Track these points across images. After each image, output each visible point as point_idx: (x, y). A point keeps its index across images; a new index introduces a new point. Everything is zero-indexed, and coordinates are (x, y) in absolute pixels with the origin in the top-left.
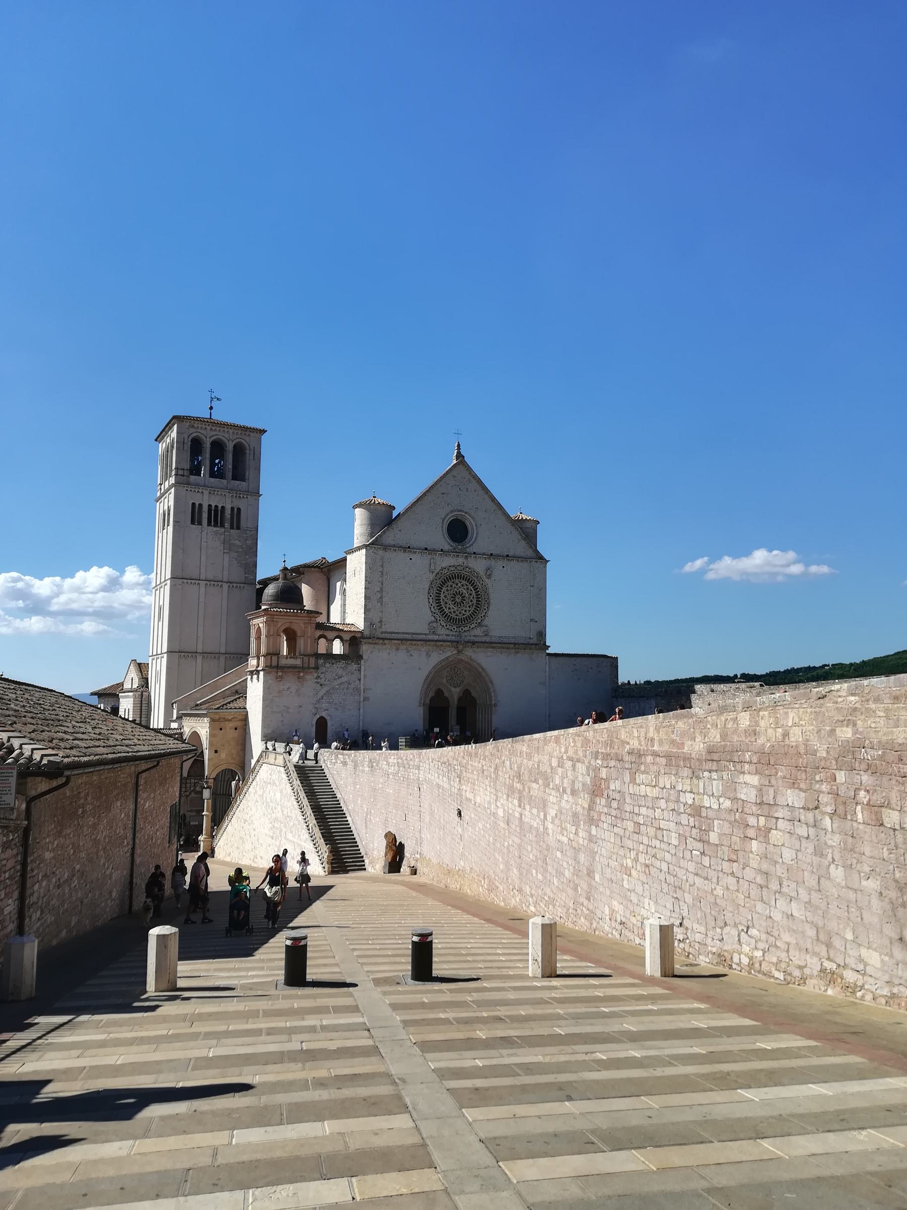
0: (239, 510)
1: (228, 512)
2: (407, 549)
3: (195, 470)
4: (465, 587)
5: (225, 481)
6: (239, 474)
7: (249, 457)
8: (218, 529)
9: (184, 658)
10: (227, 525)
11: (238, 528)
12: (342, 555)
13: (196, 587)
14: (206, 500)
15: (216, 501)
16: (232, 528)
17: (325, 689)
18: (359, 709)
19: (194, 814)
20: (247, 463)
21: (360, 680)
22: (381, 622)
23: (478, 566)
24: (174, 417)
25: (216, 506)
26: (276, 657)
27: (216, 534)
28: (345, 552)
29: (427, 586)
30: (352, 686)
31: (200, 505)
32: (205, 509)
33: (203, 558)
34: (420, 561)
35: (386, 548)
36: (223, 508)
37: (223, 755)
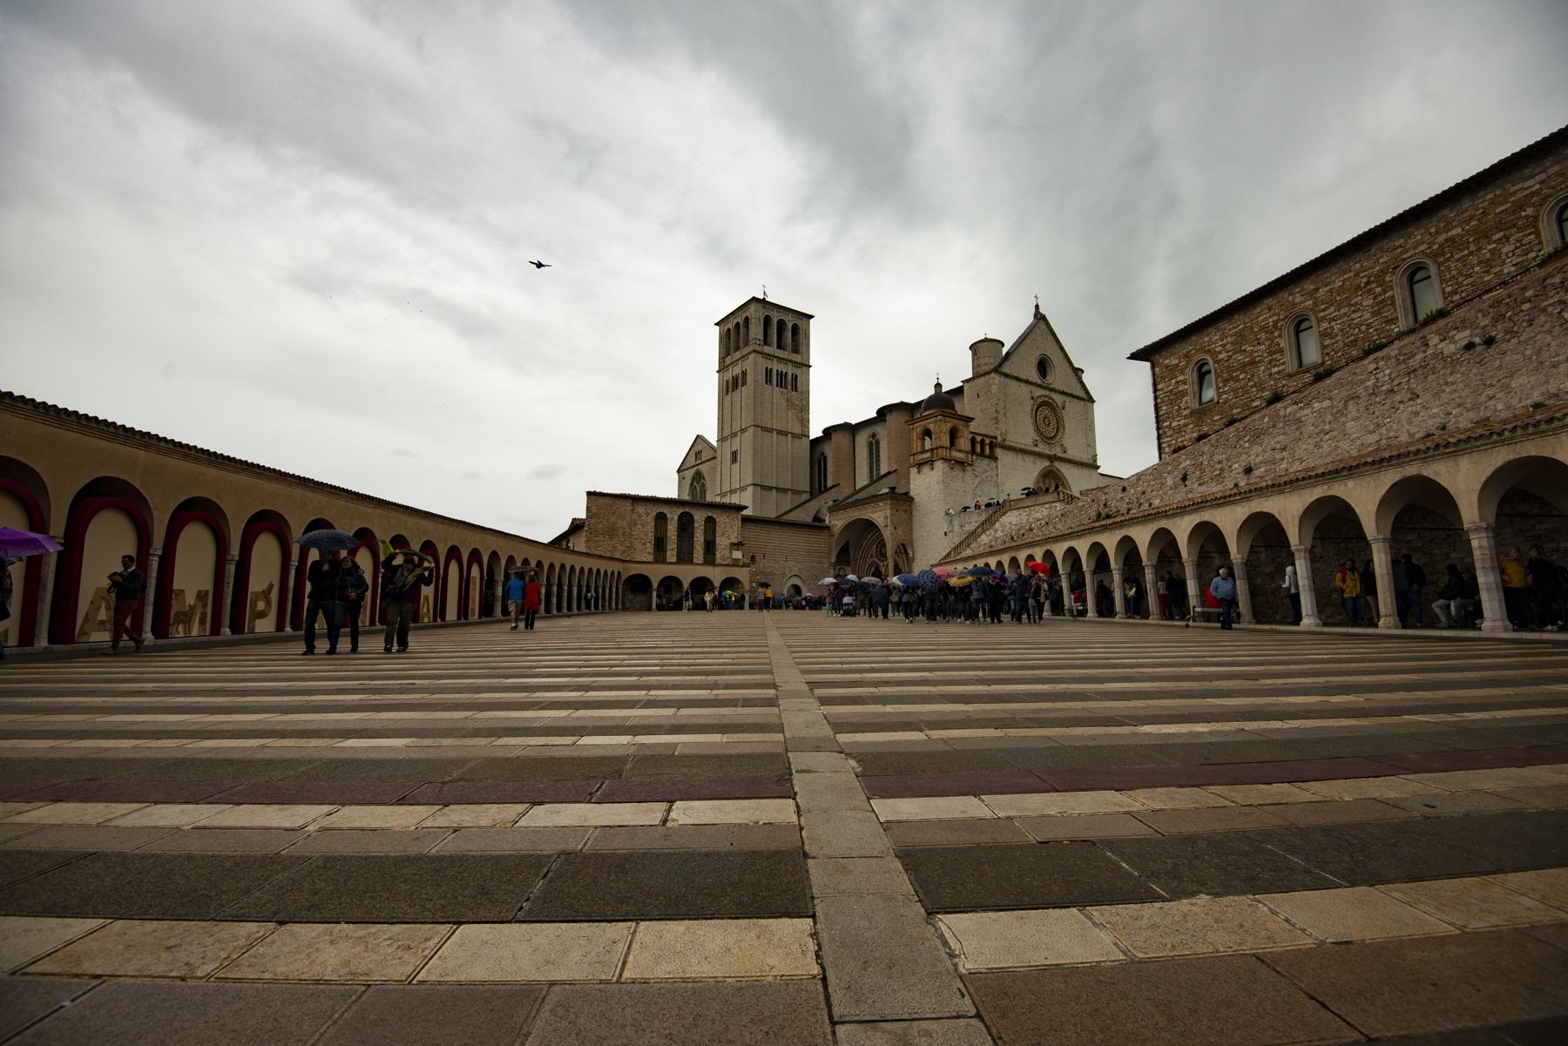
0: (796, 376)
1: (790, 377)
2: (1018, 379)
3: (766, 342)
11: (796, 391)
13: (770, 434)
14: (776, 366)
15: (782, 368)
17: (979, 479)
23: (1058, 399)
24: (754, 298)
25: (782, 372)
28: (962, 382)
29: (1029, 409)
30: (994, 480)
33: (775, 411)
35: (1006, 375)
36: (786, 373)
37: (900, 532)
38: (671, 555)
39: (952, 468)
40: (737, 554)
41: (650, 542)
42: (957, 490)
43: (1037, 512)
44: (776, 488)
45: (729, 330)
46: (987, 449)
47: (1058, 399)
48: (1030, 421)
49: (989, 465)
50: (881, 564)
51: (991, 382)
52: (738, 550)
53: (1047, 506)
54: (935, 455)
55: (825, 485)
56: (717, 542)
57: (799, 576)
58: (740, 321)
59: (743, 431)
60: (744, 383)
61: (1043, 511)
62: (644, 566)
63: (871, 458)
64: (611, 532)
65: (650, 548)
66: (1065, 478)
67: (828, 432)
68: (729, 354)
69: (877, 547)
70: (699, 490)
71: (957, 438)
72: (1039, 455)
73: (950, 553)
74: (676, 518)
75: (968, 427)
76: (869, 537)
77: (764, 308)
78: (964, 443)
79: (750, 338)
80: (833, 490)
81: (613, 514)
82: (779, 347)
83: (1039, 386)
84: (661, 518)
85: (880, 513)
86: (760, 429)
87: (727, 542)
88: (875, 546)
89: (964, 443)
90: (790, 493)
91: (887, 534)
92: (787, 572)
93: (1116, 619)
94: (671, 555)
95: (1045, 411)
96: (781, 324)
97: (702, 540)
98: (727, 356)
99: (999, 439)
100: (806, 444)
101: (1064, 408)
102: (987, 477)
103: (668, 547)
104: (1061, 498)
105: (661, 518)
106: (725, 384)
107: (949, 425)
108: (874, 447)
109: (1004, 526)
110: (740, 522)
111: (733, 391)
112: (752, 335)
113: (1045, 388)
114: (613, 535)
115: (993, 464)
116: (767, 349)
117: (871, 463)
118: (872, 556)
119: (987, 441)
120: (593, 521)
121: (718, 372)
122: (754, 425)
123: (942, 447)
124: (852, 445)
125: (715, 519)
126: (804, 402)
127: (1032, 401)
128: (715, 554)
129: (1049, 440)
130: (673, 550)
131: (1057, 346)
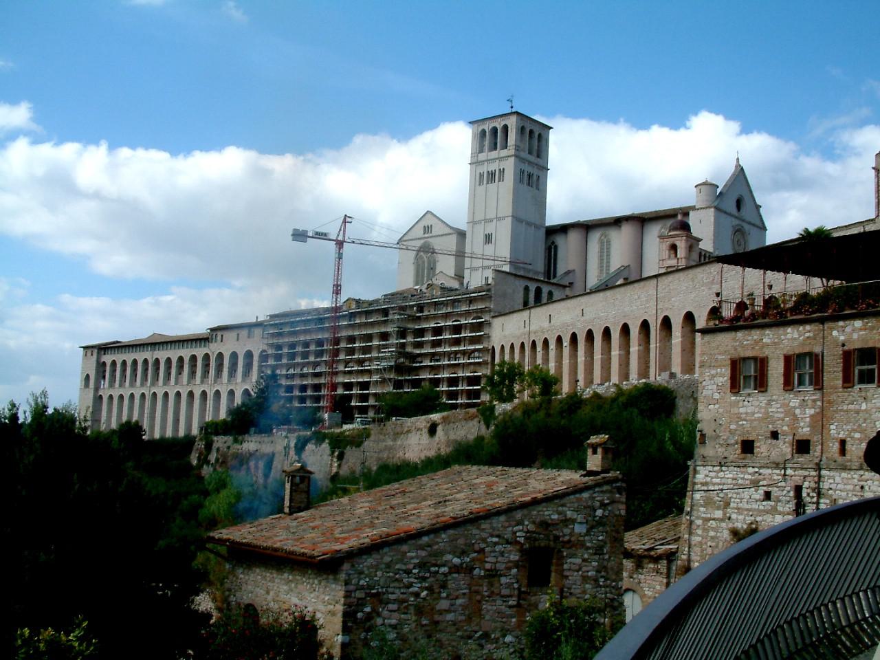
1: (535, 178)
2: (725, 213)
6: (538, 156)
10: (534, 186)
14: (528, 169)
23: (746, 227)
32: (526, 174)
34: (729, 219)
45: (483, 132)
58: (498, 127)
59: (499, 219)
67: (564, 229)
70: (426, 259)
74: (534, 290)
75: (698, 245)
77: (522, 119)
78: (695, 256)
80: (571, 274)
83: (736, 217)
95: (738, 236)
96: (531, 132)
100: (542, 233)
105: (527, 289)
107: (689, 243)
119: (707, 255)
121: (470, 164)
127: (731, 229)
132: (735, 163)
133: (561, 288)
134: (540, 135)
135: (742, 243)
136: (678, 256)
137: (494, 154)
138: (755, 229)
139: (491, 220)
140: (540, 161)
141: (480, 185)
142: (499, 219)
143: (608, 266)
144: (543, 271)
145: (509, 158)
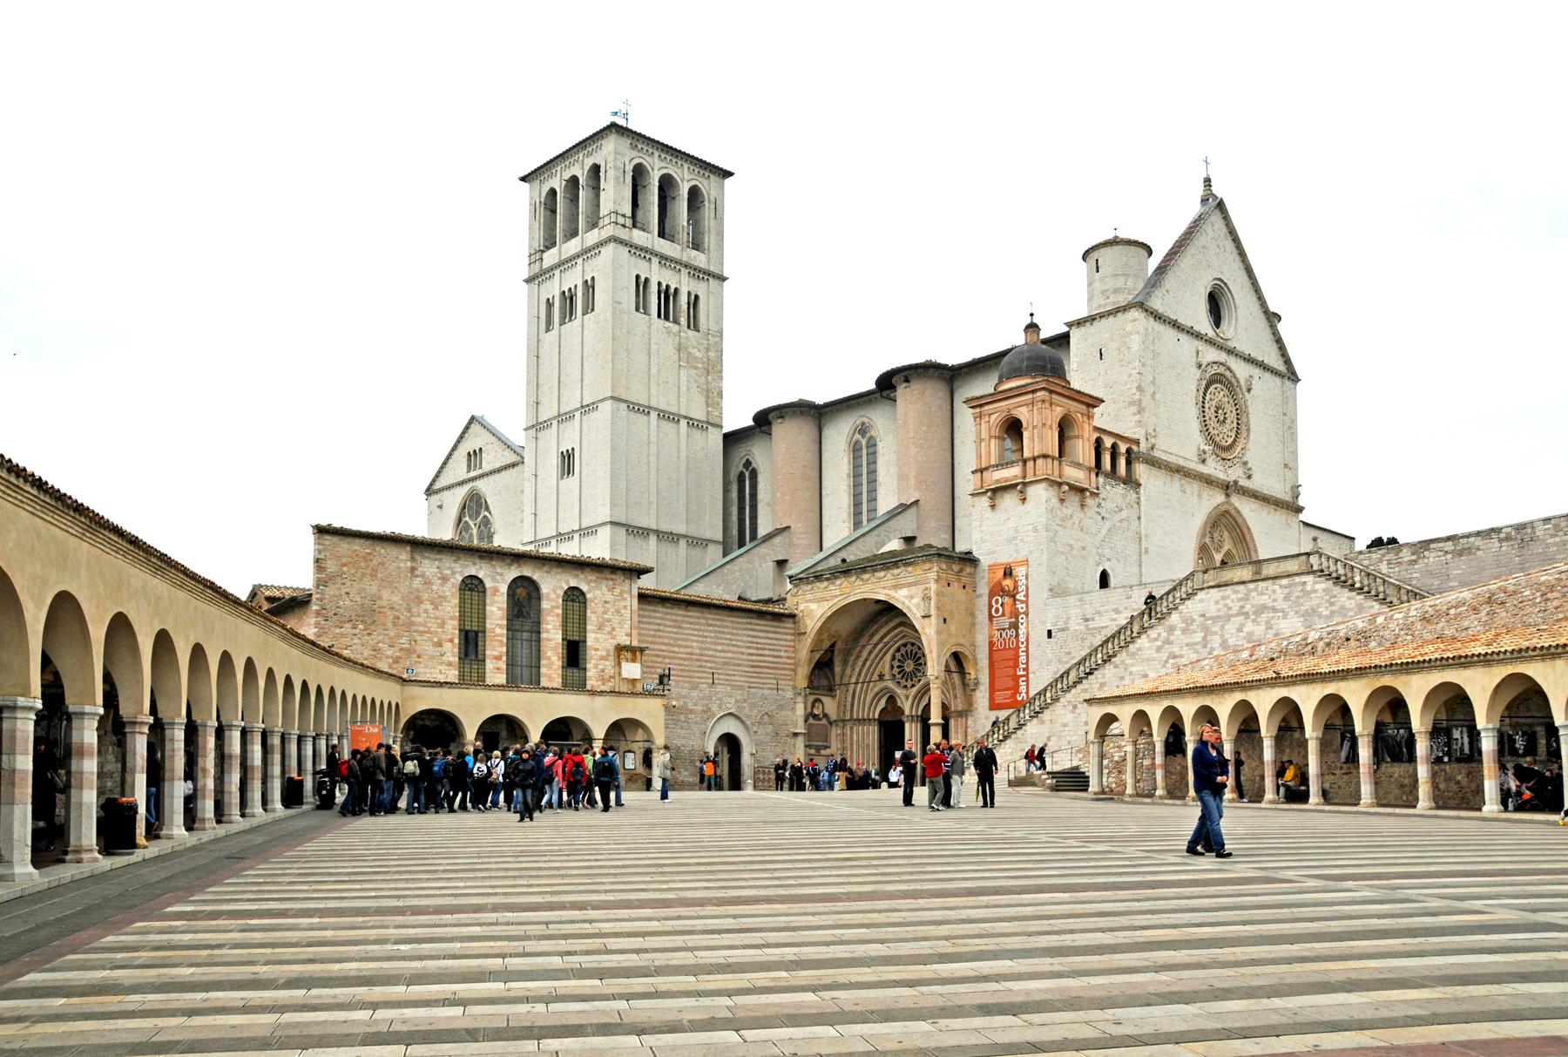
0: (697, 297)
1: (683, 299)
4: (1226, 399)
5: (678, 247)
7: (707, 212)
8: (671, 325)
9: (632, 536)
11: (697, 329)
12: (1066, 329)
13: (642, 418)
15: (670, 279)
16: (689, 327)
17: (1107, 525)
18: (1140, 566)
19: (813, 751)
20: (707, 223)
21: (1139, 518)
22: (1154, 430)
23: (1241, 370)
25: (668, 286)
26: (1056, 463)
27: (668, 333)
31: (647, 280)
32: (654, 288)
33: (654, 371)
36: (676, 290)
37: (953, 628)
38: (495, 671)
39: (1062, 501)
40: (632, 670)
41: (451, 641)
42: (1071, 546)
43: (1263, 594)
44: (657, 532)
45: (553, 192)
46: (1122, 462)
47: (1241, 370)
48: (1194, 412)
49: (1124, 496)
50: (899, 691)
51: (1129, 327)
52: (634, 661)
53: (1285, 582)
54: (1030, 470)
55: (754, 536)
56: (589, 642)
57: (737, 717)
59: (587, 409)
60: (589, 307)
61: (1274, 591)
62: (446, 693)
63: (856, 475)
64: (368, 616)
65: (451, 651)
66: (1249, 529)
67: (764, 420)
68: (554, 244)
69: (894, 658)
71: (1070, 438)
72: (1208, 481)
73: (1067, 672)
74: (504, 589)
75: (1090, 417)
76: (876, 638)
78: (1083, 450)
79: (603, 211)
80: (777, 540)
81: (373, 576)
82: (662, 234)
83: (1210, 342)
84: (473, 586)
85: (913, 589)
86: (624, 406)
87: (610, 644)
88: (888, 657)
89: (1083, 450)
90: (683, 543)
91: (929, 633)
92: (715, 708)
93: (1263, 805)
94: (495, 671)
95: (1218, 395)
97: (559, 637)
98: (548, 248)
99: (1143, 446)
100: (715, 441)
101: (1249, 390)
102: (1121, 521)
103: (488, 652)
104: (1315, 568)
105: (473, 586)
106: (543, 307)
108: (864, 454)
109: (1188, 621)
110: (635, 601)
111: (562, 323)
112: (606, 206)
113: (1221, 348)
114: (374, 622)
115: (1132, 495)
116: (638, 237)
117: (857, 485)
118: (881, 676)
119: (1123, 448)
120: (331, 590)
122: (613, 398)
123: (1045, 456)
124: (817, 454)
125: (583, 594)
126: (712, 354)
128: (585, 669)
129: (1223, 450)
130: (498, 658)
131: (1241, 265)
132: (1199, 190)
133: (619, 577)
134: (694, 193)
135: (1232, 417)
136: (1027, 454)
137: (573, 246)
138: (1268, 375)
139: (569, 416)
140: (699, 259)
141: (548, 330)
142: (587, 409)
143: (872, 510)
144: (719, 536)
145: (603, 250)
